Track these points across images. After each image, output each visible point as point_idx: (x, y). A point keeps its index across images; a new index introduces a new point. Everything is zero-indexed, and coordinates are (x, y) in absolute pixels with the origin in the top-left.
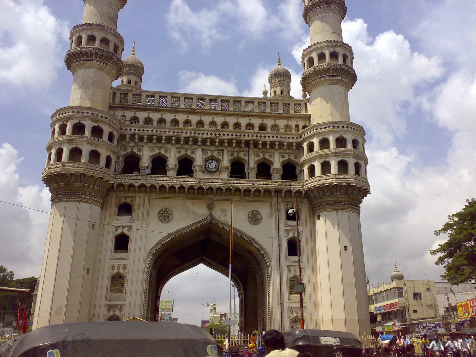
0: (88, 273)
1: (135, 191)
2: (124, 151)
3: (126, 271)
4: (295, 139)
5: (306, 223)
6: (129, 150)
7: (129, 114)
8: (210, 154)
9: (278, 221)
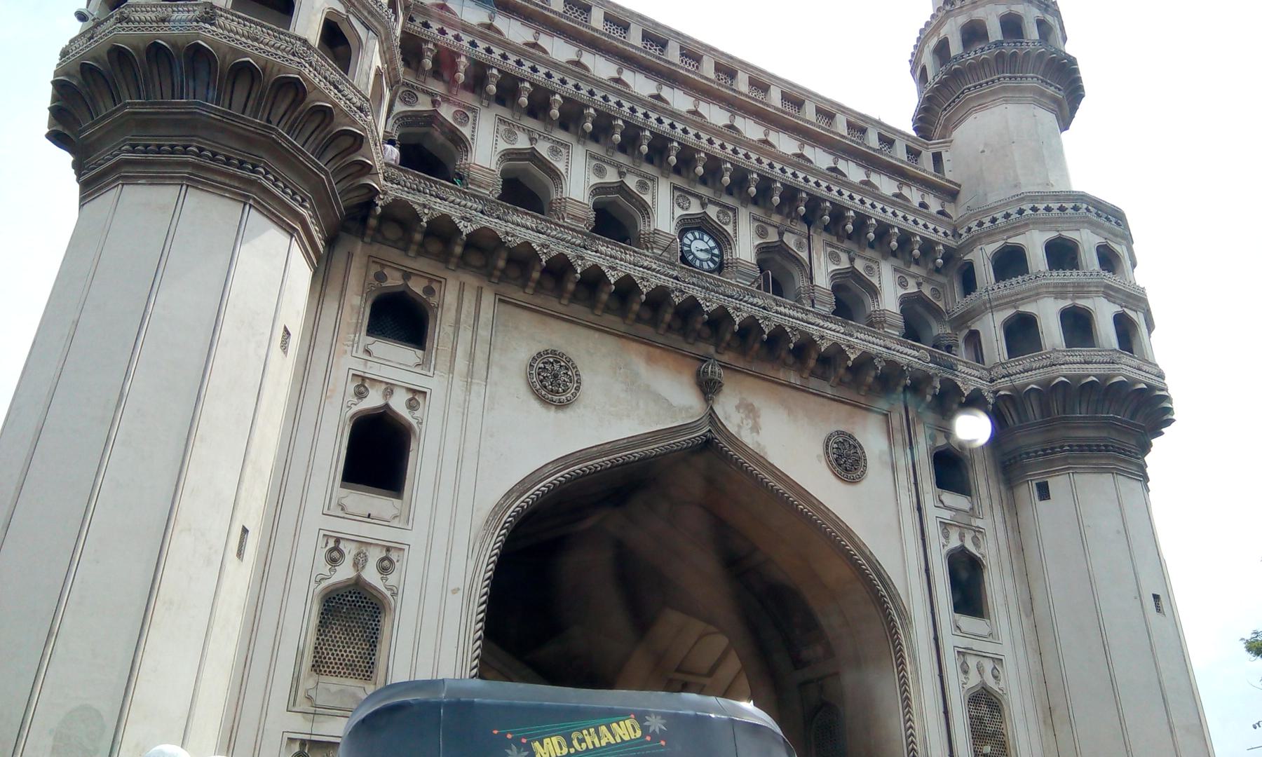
1: (444, 257)
3: (392, 579)
5: (991, 506)
6: (423, 105)
8: (695, 208)
9: (916, 484)
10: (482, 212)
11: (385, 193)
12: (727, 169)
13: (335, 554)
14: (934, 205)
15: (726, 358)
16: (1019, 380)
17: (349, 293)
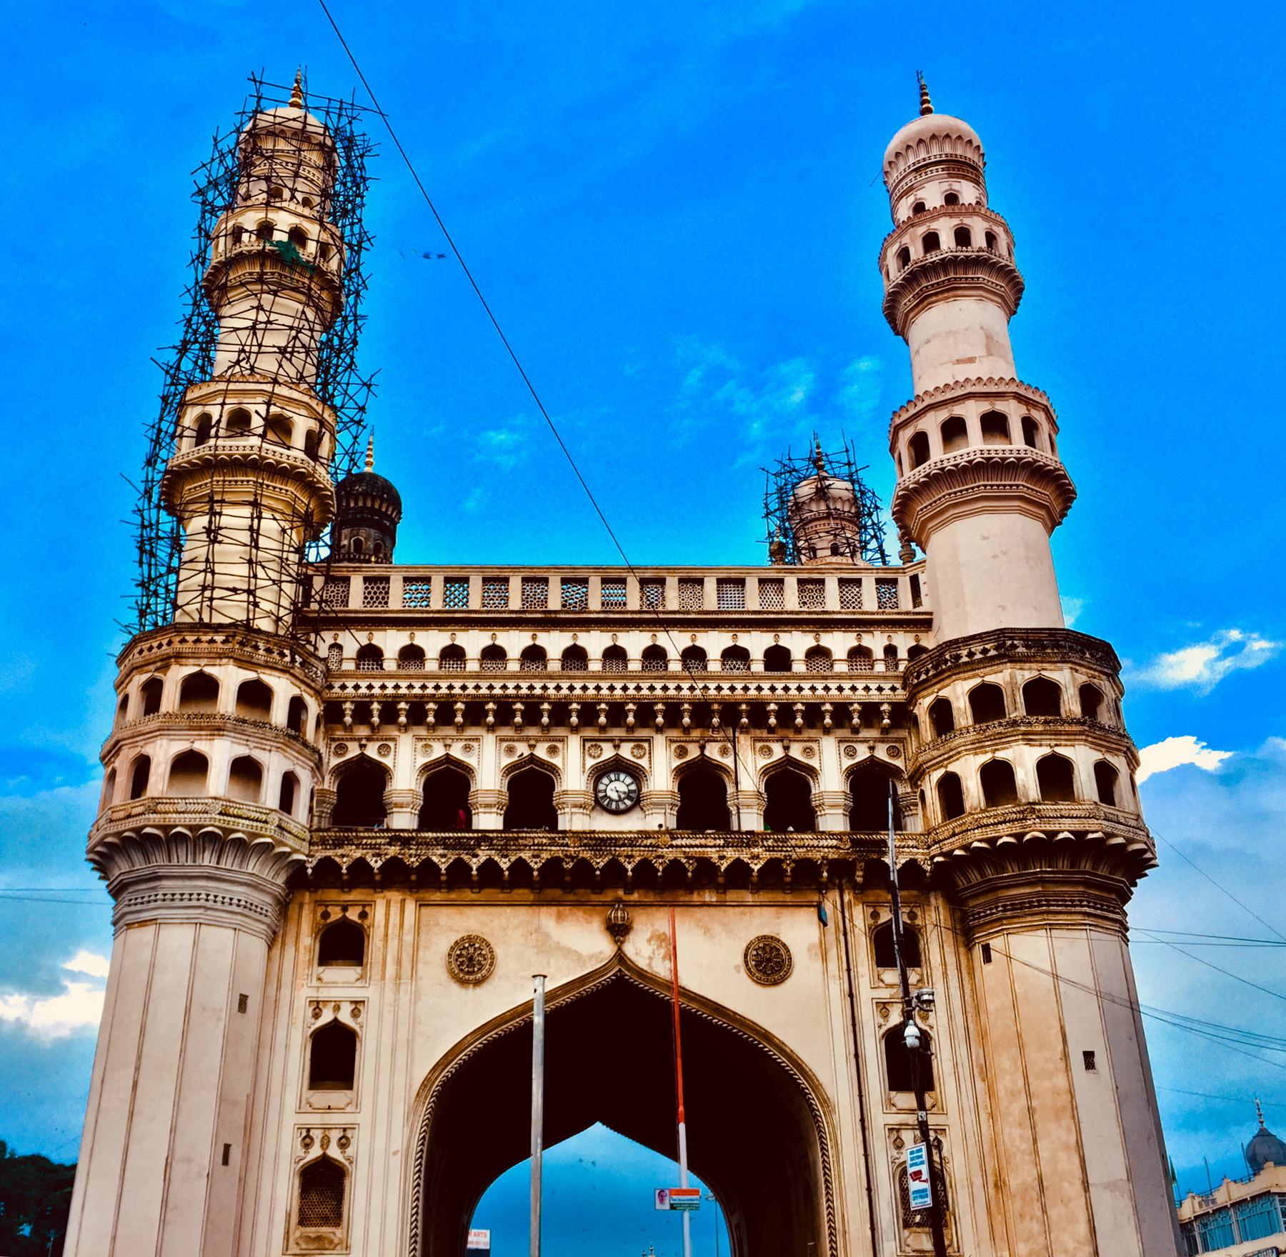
0: (226, 1161)
2: (337, 754)
3: (349, 1151)
4: (887, 692)
6: (353, 751)
7: (351, 642)
8: (608, 752)
12: (630, 710)
13: (308, 1140)
14: (904, 642)
15: (635, 897)
17: (302, 936)
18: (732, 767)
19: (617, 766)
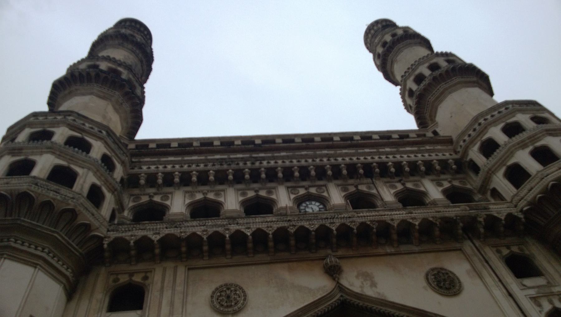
2: (134, 201)
8: (302, 192)
9: (500, 281)
10: (167, 228)
11: (109, 237)
12: (311, 169)
15: (340, 253)
16: (530, 197)
18: (377, 193)
19: (309, 198)
